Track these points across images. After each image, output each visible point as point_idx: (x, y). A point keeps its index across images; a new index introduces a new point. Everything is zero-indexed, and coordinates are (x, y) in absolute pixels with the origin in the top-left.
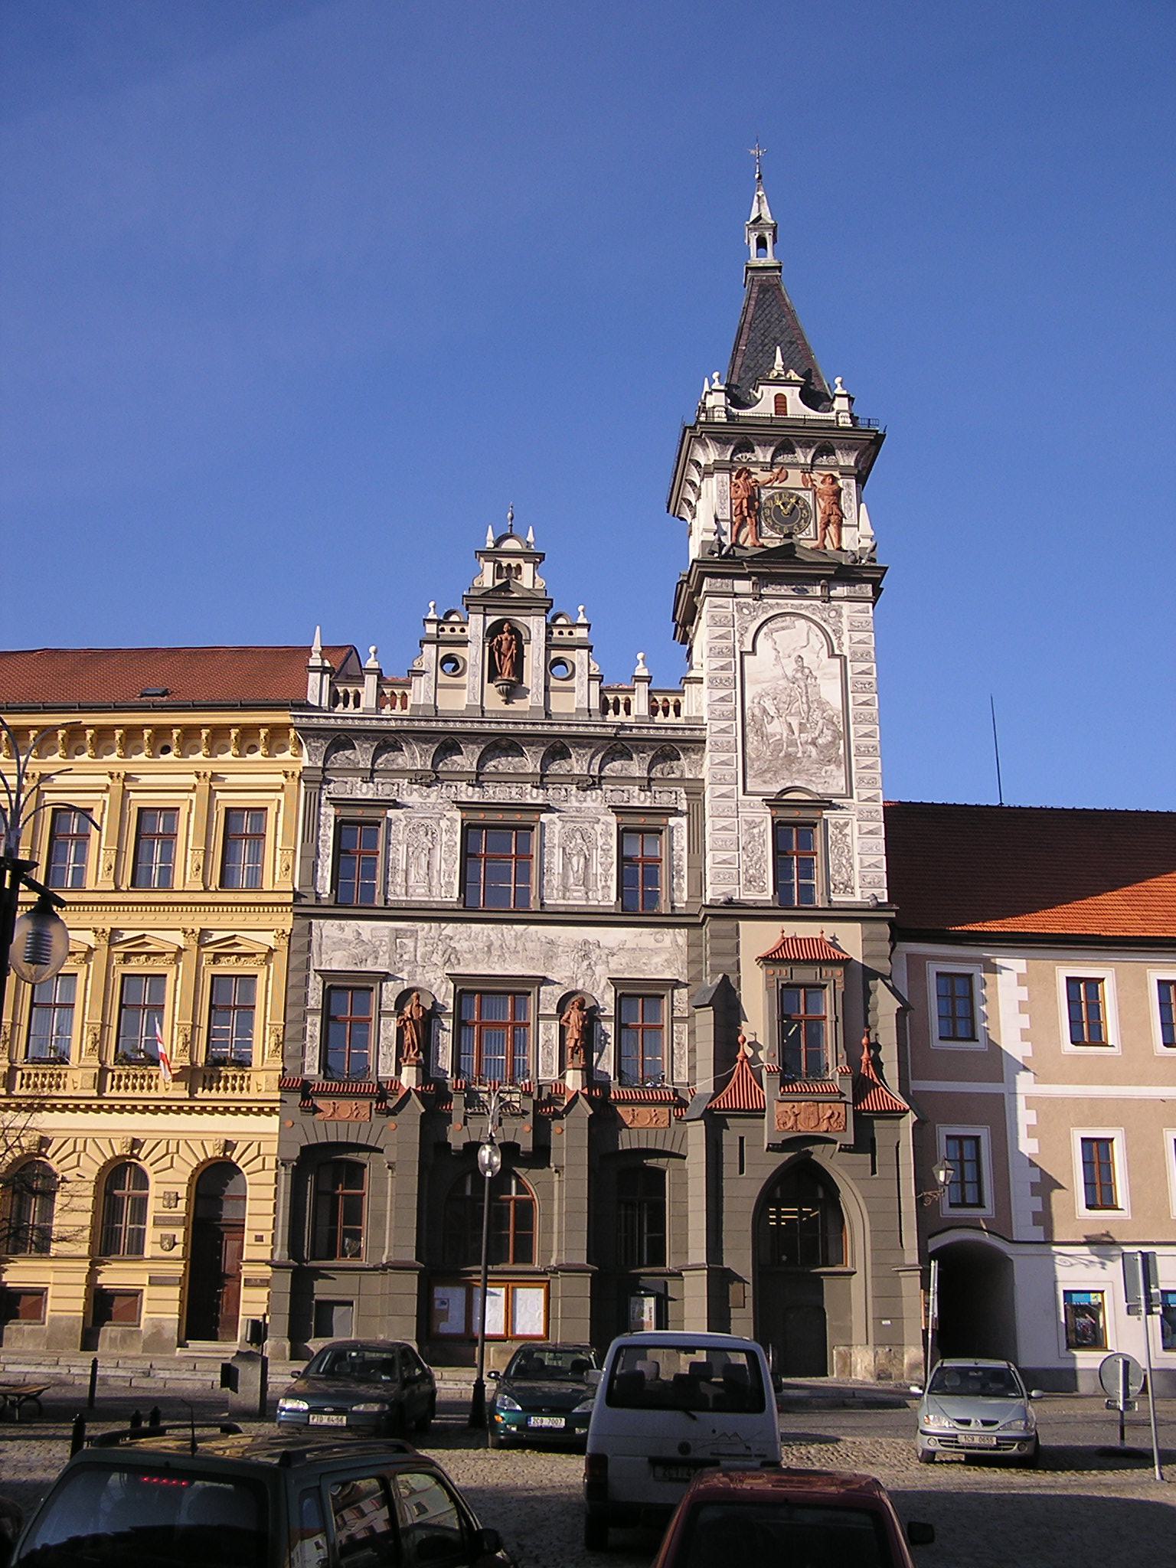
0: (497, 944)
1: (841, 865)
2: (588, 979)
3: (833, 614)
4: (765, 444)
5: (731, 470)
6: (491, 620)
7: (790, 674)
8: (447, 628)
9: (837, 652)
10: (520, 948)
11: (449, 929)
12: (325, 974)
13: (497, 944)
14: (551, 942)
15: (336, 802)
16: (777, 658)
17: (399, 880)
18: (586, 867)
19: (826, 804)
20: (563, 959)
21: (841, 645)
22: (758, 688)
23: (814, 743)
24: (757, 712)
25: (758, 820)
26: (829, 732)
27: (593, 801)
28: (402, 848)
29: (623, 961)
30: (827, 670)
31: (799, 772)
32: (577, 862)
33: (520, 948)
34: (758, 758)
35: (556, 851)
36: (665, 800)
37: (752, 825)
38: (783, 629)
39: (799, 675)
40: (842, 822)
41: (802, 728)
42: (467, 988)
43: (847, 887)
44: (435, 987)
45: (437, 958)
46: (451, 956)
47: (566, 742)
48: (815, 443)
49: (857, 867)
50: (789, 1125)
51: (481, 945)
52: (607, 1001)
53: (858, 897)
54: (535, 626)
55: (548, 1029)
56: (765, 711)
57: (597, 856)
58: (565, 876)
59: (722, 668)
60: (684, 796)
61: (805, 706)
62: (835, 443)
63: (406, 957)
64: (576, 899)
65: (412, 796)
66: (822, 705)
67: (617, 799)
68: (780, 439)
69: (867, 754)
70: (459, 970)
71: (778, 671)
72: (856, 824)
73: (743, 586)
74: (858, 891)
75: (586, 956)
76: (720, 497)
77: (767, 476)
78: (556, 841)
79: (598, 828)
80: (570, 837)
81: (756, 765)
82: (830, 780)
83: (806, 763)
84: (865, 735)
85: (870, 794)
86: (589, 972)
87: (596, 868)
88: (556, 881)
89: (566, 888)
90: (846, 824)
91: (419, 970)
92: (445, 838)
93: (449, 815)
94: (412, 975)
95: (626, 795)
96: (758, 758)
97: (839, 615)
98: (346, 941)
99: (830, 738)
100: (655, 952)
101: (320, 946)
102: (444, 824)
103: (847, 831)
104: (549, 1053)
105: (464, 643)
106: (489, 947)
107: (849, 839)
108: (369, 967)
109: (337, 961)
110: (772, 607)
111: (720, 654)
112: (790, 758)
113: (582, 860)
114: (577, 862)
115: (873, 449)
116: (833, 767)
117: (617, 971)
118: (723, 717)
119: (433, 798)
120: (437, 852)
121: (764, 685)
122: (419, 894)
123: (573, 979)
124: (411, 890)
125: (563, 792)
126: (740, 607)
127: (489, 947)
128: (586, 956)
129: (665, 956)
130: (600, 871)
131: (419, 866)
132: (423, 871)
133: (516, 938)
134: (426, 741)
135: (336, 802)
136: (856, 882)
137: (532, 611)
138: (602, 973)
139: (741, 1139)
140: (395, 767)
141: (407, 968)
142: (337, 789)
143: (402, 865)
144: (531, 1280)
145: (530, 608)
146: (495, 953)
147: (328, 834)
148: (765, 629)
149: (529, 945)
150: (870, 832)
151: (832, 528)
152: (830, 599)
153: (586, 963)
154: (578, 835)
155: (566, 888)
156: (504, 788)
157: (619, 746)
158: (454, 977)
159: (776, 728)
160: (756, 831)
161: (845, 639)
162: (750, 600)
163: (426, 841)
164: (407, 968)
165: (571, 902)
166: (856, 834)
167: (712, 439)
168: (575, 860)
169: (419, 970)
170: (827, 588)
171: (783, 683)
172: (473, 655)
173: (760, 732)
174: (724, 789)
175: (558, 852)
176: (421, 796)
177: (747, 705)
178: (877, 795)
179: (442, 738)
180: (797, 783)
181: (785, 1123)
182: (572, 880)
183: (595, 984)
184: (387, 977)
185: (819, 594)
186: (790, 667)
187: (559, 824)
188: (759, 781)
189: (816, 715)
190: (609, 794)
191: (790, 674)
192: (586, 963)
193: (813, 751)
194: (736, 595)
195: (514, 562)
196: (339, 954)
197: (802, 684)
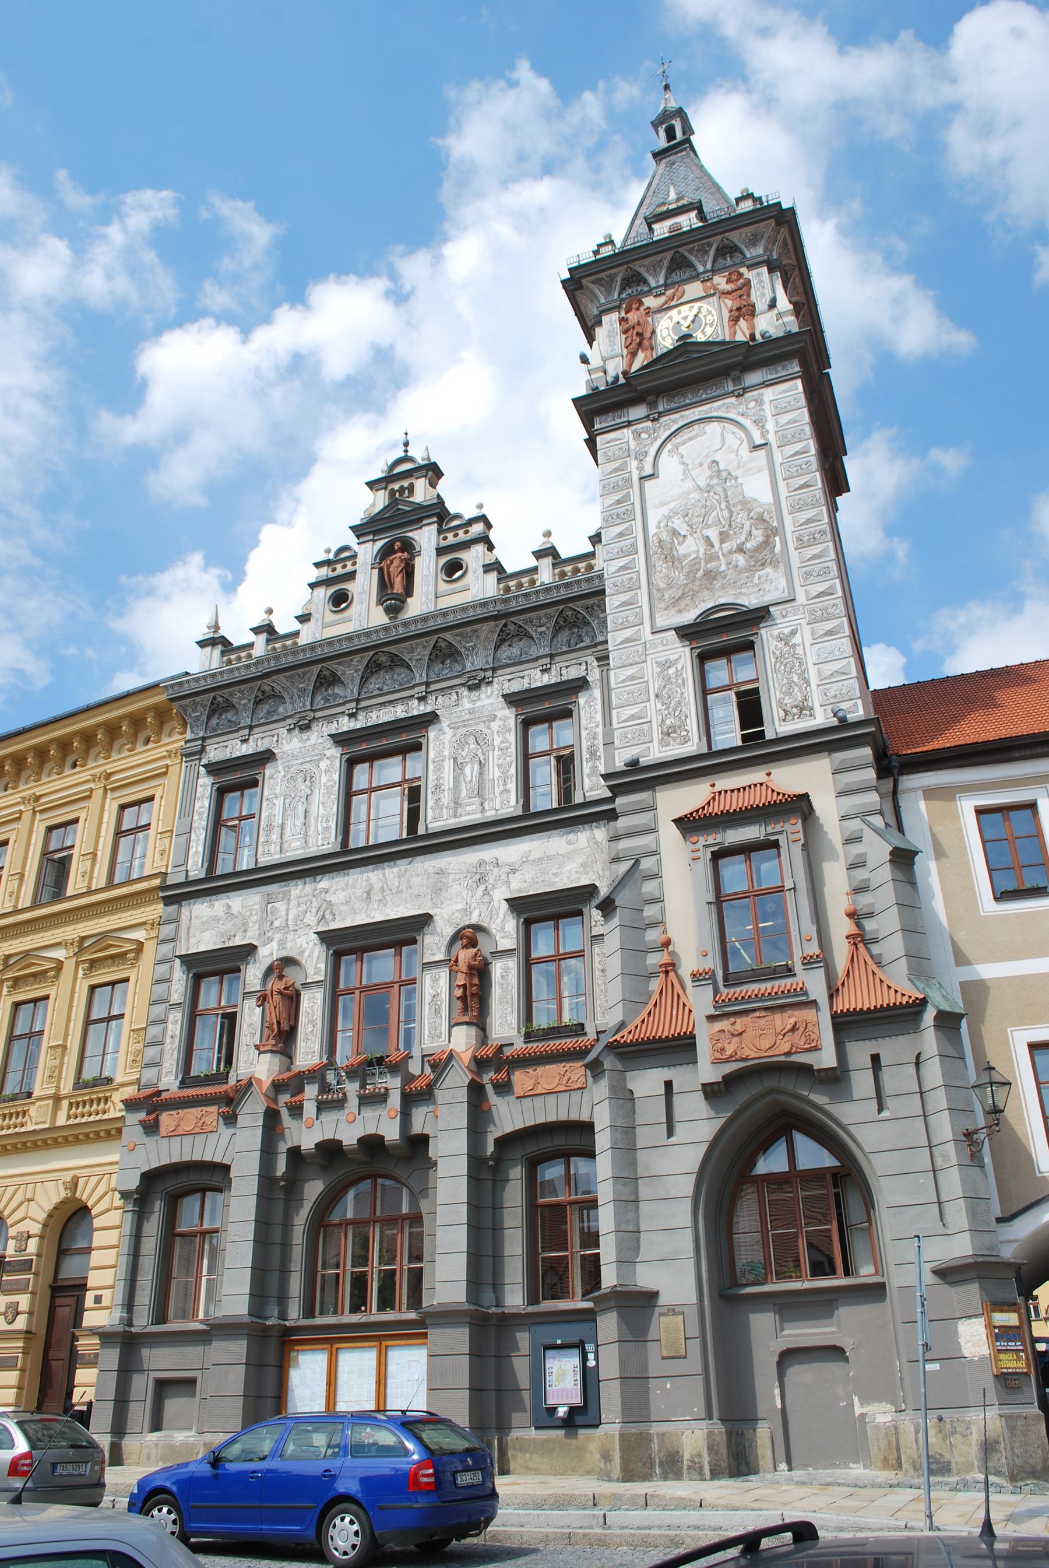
0: (377, 886)
1: (791, 684)
2: (484, 907)
3: (752, 404)
4: (654, 269)
5: (618, 308)
6: (380, 544)
7: (702, 483)
8: (339, 567)
9: (759, 441)
10: (403, 887)
11: (325, 883)
12: (189, 961)
13: (377, 886)
14: (441, 872)
15: (213, 769)
16: (686, 472)
17: (275, 837)
18: (481, 774)
19: (760, 615)
20: (455, 889)
21: (764, 434)
22: (665, 511)
23: (740, 550)
24: (665, 536)
25: (673, 658)
26: (760, 532)
27: (490, 698)
28: (279, 802)
29: (528, 877)
30: (748, 466)
31: (723, 587)
32: (470, 771)
33: (403, 887)
34: (669, 586)
35: (446, 764)
36: (573, 673)
37: (666, 665)
38: (691, 439)
39: (715, 481)
40: (786, 631)
41: (724, 537)
42: (345, 944)
43: (804, 709)
44: (306, 954)
45: (311, 919)
46: (327, 909)
47: (448, 636)
48: (710, 245)
49: (814, 681)
50: (728, 1053)
51: (359, 892)
52: (505, 931)
53: (821, 719)
54: (426, 538)
55: (435, 981)
56: (674, 533)
57: (494, 758)
58: (456, 788)
59: (619, 502)
60: (595, 663)
61: (726, 513)
62: (735, 237)
63: (276, 924)
64: (471, 815)
65: (290, 745)
66: (746, 504)
67: (516, 686)
68: (669, 255)
69: (814, 541)
70: (333, 926)
71: (689, 485)
72: (806, 630)
73: (638, 412)
74: (818, 711)
75: (481, 880)
76: (609, 336)
77: (661, 300)
78: (446, 753)
79: (495, 726)
80: (461, 744)
81: (667, 595)
82: (766, 586)
83: (731, 574)
84: (808, 521)
85: (822, 587)
86: (486, 899)
87: (494, 772)
88: (446, 798)
89: (457, 803)
90: (793, 633)
91: (290, 936)
92: (324, 779)
93: (329, 753)
94: (282, 943)
95: (526, 681)
96: (669, 586)
97: (759, 402)
98: (216, 919)
99: (761, 539)
100: (568, 856)
101: (188, 929)
102: (323, 765)
103: (797, 639)
104: (437, 1011)
105: (351, 576)
106: (368, 893)
107: (799, 650)
108: (238, 941)
109: (204, 941)
110: (675, 422)
111: (616, 487)
112: (711, 576)
113: (476, 767)
114: (470, 771)
115: (784, 231)
116: (768, 570)
117: (519, 891)
118: (623, 553)
119: (312, 741)
120: (315, 799)
121: (671, 506)
122: (295, 850)
123: (467, 911)
124: (285, 846)
125: (454, 696)
126: (637, 435)
127: (368, 893)
128: (481, 880)
129: (580, 860)
130: (497, 774)
131: (295, 816)
132: (299, 823)
133: (400, 876)
134: (302, 677)
135: (213, 769)
136: (816, 700)
137: (425, 522)
138: (500, 894)
139: (669, 1085)
140: (276, 718)
141: (278, 937)
142: (216, 753)
143: (278, 820)
144: (411, 1333)
145: (420, 520)
146: (375, 897)
147: (203, 804)
148: (669, 446)
149: (415, 880)
150: (830, 633)
151: (742, 323)
152: (745, 390)
153: (482, 888)
154: (471, 740)
155: (457, 803)
156: (390, 708)
157: (511, 627)
158: (326, 937)
159: (690, 547)
160: (671, 671)
161: (770, 426)
162: (649, 424)
163: (303, 788)
164: (278, 937)
165: (463, 819)
166: (808, 640)
167: (593, 282)
168: (468, 770)
169: (290, 936)
170: (737, 380)
171: (696, 495)
172: (364, 586)
173: (671, 558)
174: (627, 633)
175: (448, 765)
176: (301, 740)
177: (652, 530)
178: (832, 587)
179: (315, 669)
180: (722, 601)
181: (723, 1049)
182: (464, 793)
183: (492, 913)
184: (249, 950)
185: (731, 388)
186: (702, 477)
187: (449, 733)
188: (673, 611)
189: (741, 518)
190: (506, 685)
191: (702, 483)
192: (482, 888)
193: (741, 560)
194: (629, 424)
195: (406, 483)
196: (207, 935)
197: (719, 490)
